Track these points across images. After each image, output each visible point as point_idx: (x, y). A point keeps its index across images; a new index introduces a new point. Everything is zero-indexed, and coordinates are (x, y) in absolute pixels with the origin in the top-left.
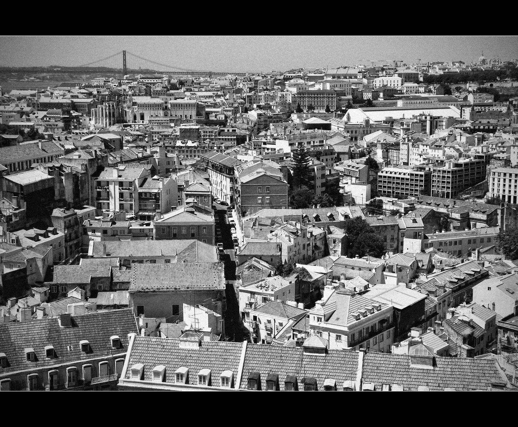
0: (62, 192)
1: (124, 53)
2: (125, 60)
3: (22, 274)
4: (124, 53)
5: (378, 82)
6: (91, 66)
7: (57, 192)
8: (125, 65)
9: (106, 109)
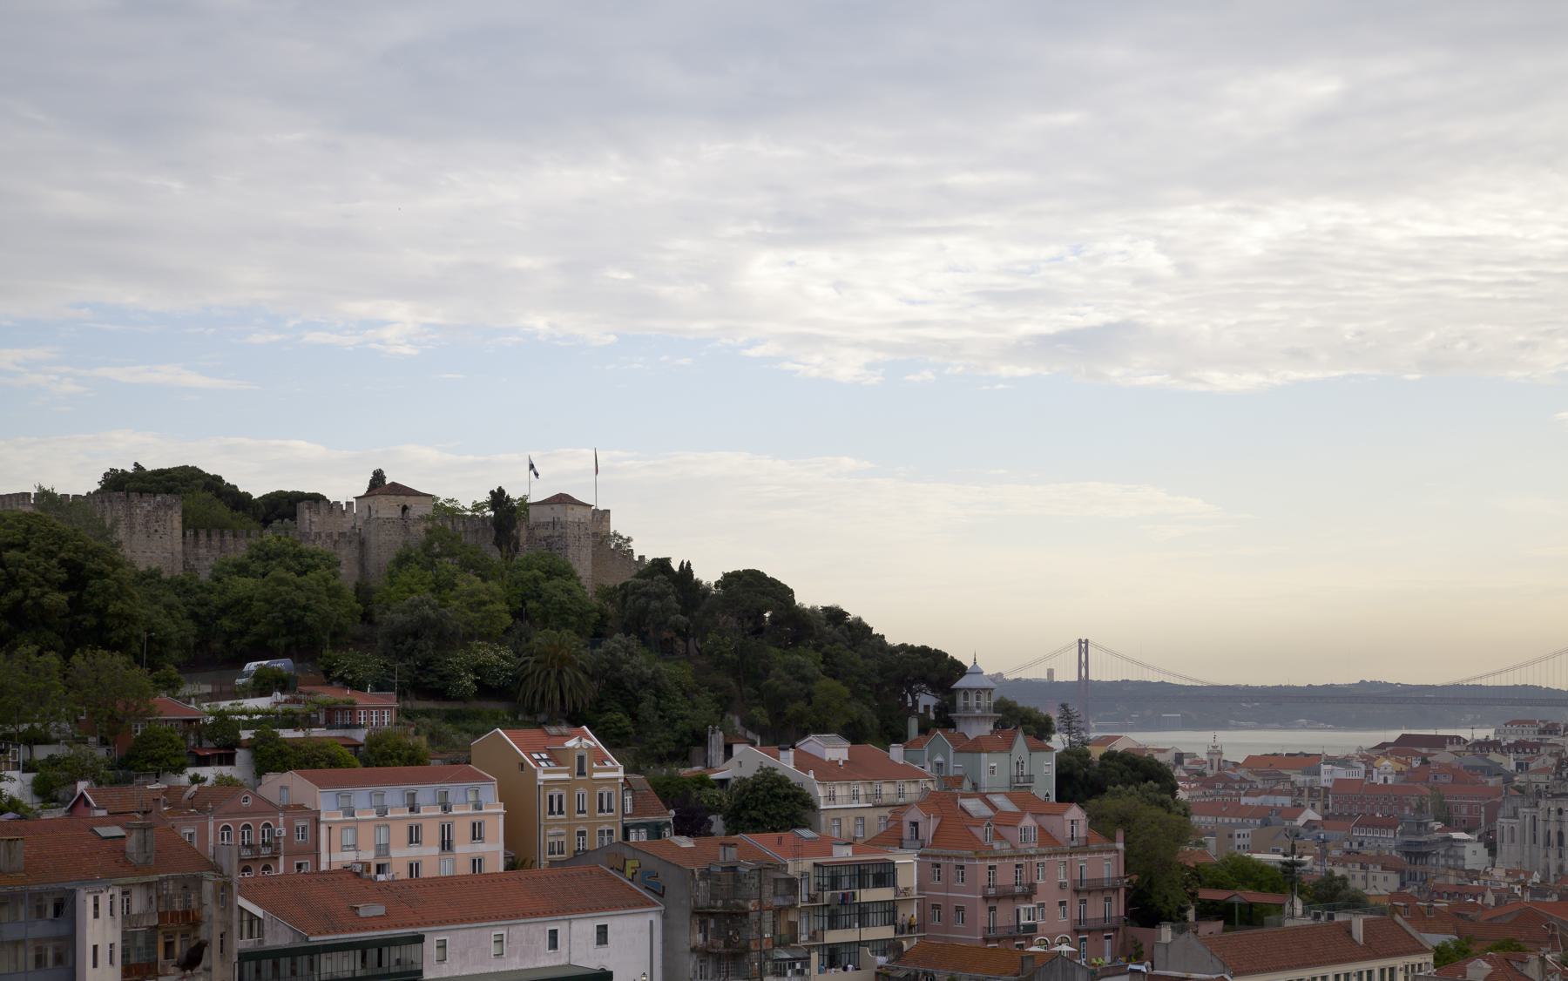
6: (1484, 682)
9: (1546, 821)
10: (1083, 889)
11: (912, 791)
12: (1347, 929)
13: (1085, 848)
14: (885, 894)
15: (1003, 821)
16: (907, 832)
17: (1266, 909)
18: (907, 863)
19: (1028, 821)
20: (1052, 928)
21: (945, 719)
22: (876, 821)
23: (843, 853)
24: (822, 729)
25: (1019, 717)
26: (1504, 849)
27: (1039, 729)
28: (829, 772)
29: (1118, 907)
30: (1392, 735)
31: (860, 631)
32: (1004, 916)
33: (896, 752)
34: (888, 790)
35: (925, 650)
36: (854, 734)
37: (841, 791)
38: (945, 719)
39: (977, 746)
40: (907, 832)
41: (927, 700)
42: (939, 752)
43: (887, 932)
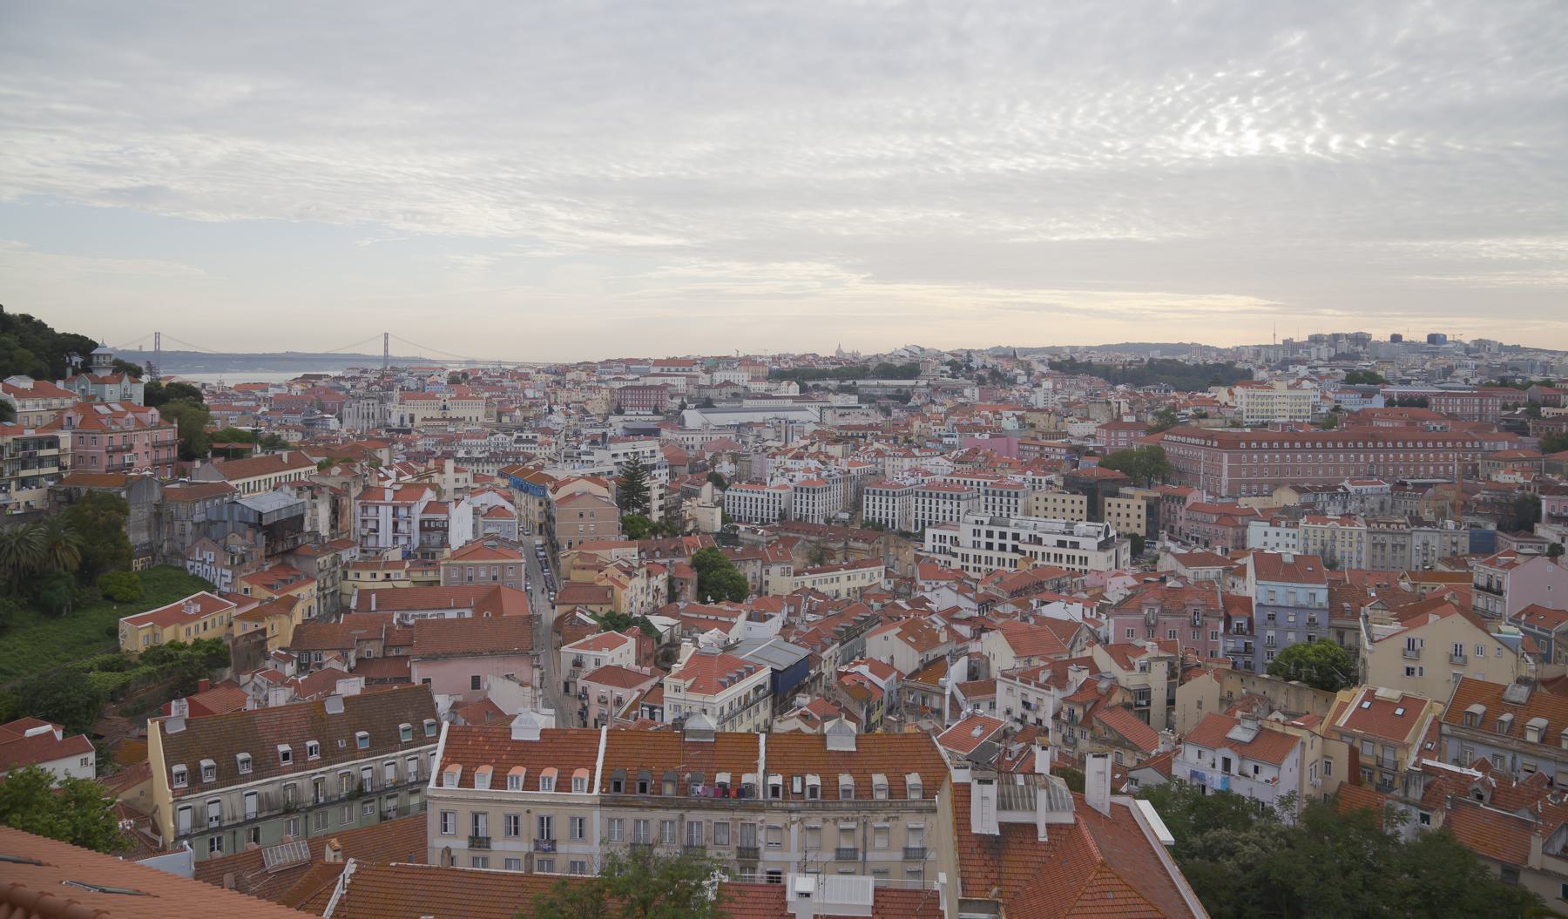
0: (314, 522)
1: (386, 335)
2: (386, 345)
3: (260, 637)
4: (386, 335)
5: (719, 377)
7: (306, 522)
8: (386, 351)
10: (157, 446)
11: (68, 402)
12: (280, 457)
13: (158, 427)
14: (54, 452)
15: (116, 416)
16: (65, 421)
17: (243, 451)
18: (66, 438)
19: (130, 415)
20: (142, 464)
21: (87, 368)
22: (48, 417)
23: (30, 433)
24: (18, 372)
25: (125, 368)
26: (348, 422)
27: (136, 373)
28: (21, 394)
29: (174, 453)
30: (300, 375)
31: (40, 326)
32: (117, 460)
33: (60, 384)
34: (55, 403)
35: (76, 336)
36: (36, 375)
37: (29, 403)
38: (87, 368)
39: (104, 381)
40: (65, 421)
41: (77, 359)
42: (84, 384)
43: (55, 470)
